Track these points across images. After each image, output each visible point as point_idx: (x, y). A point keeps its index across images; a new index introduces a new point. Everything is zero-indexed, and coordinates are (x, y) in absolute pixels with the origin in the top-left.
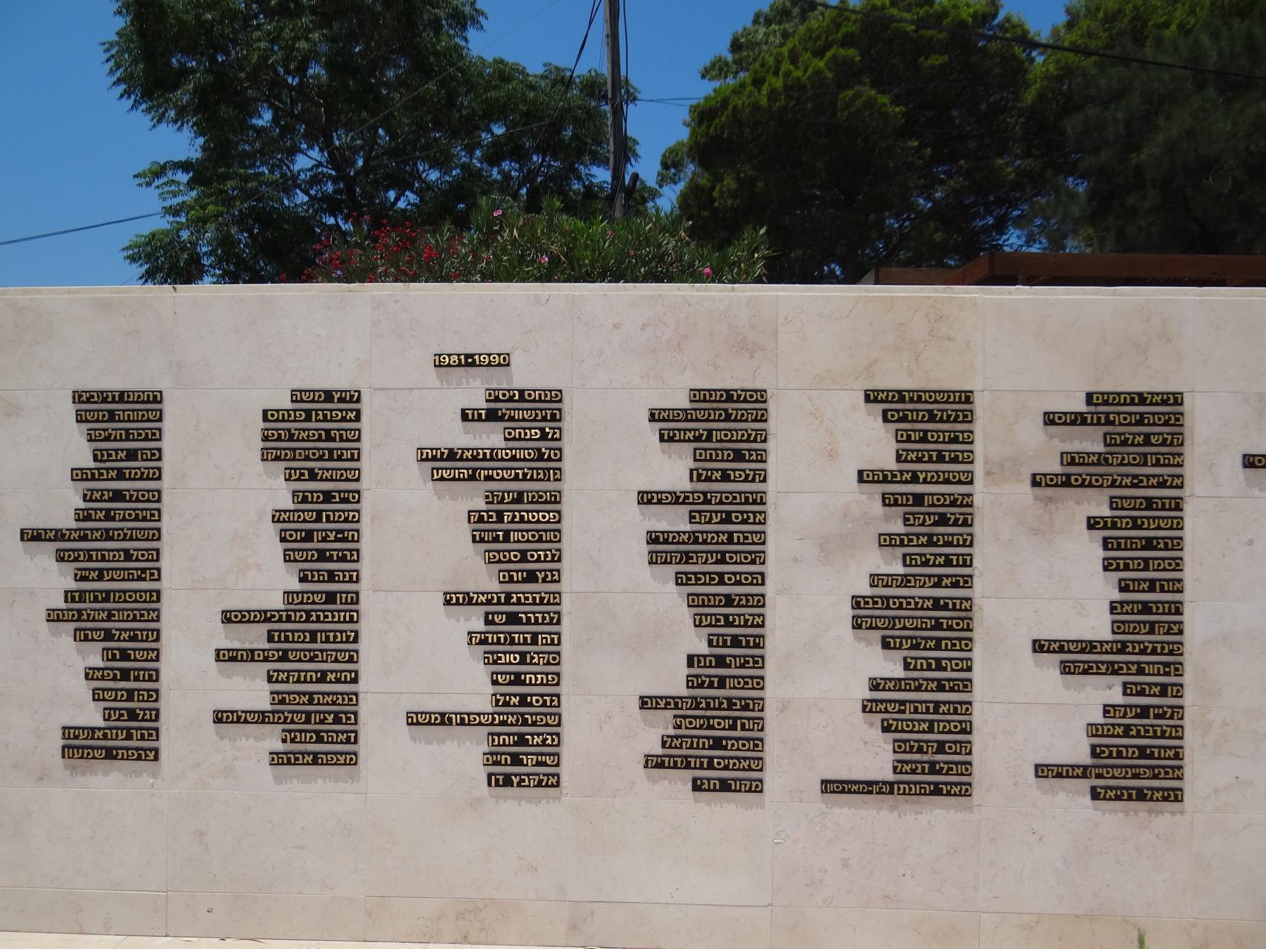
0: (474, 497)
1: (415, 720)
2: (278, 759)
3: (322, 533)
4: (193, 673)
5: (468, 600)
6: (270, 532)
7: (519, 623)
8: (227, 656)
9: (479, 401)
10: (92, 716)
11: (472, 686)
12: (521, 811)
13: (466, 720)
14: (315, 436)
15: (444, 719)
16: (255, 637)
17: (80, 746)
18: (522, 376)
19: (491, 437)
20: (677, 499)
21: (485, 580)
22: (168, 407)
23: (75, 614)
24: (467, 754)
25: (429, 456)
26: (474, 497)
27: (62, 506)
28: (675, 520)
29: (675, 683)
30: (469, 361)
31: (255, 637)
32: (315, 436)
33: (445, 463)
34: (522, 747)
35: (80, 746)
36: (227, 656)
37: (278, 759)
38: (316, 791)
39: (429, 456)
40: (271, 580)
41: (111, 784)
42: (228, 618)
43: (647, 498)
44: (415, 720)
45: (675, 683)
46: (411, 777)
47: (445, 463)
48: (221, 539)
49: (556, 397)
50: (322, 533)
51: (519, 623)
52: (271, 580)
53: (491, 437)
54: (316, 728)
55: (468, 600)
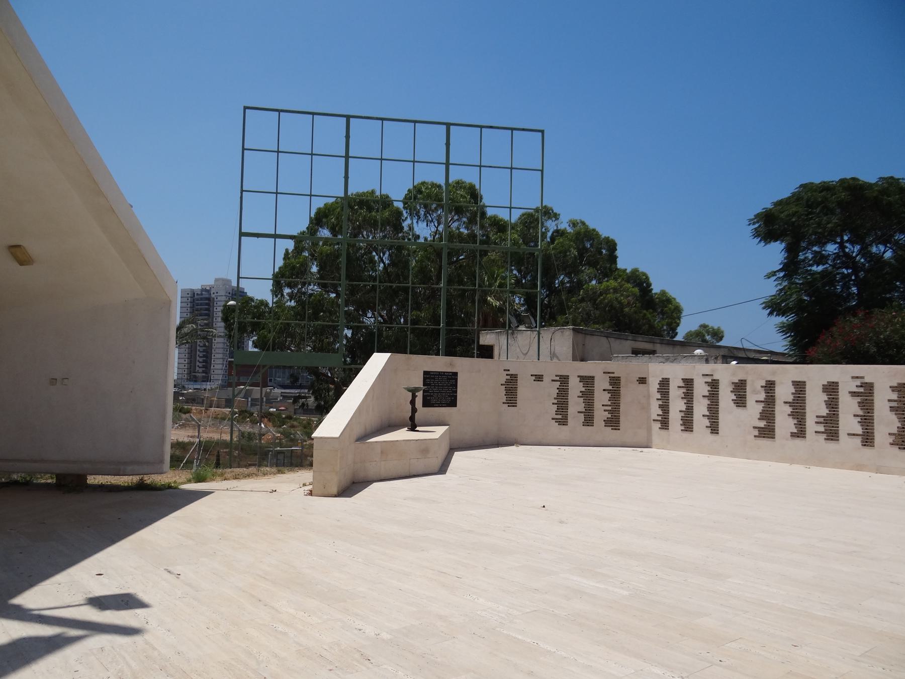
0: (859, 399)
1: (849, 434)
2: (826, 439)
3: (833, 404)
4: (811, 425)
5: (858, 416)
6: (824, 404)
7: (867, 420)
8: (817, 423)
9: (859, 384)
10: (795, 431)
11: (859, 430)
12: (867, 451)
13: (857, 435)
14: (831, 389)
15: (854, 435)
16: (822, 420)
17: (793, 435)
18: (867, 380)
19: (861, 390)
20: (895, 401)
21: (861, 413)
22: (807, 384)
23: (792, 415)
24: (858, 441)
25: (850, 392)
26: (859, 399)
27: (790, 398)
28: (894, 404)
29: (895, 431)
30: (857, 377)
31: (822, 420)
32: (831, 389)
33: (854, 394)
34: (868, 439)
35: (793, 435)
36: (817, 423)
37: (826, 439)
38: (832, 445)
39: (850, 392)
40: (824, 411)
41: (798, 442)
42: (817, 417)
43: (889, 401)
44: (849, 434)
45: (895, 431)
46: (848, 444)
47: (854, 394)
48: (816, 405)
49: (872, 384)
50: (833, 404)
51: (867, 420)
52: (824, 411)
53: (861, 390)
54: (832, 434)
55: (858, 416)
